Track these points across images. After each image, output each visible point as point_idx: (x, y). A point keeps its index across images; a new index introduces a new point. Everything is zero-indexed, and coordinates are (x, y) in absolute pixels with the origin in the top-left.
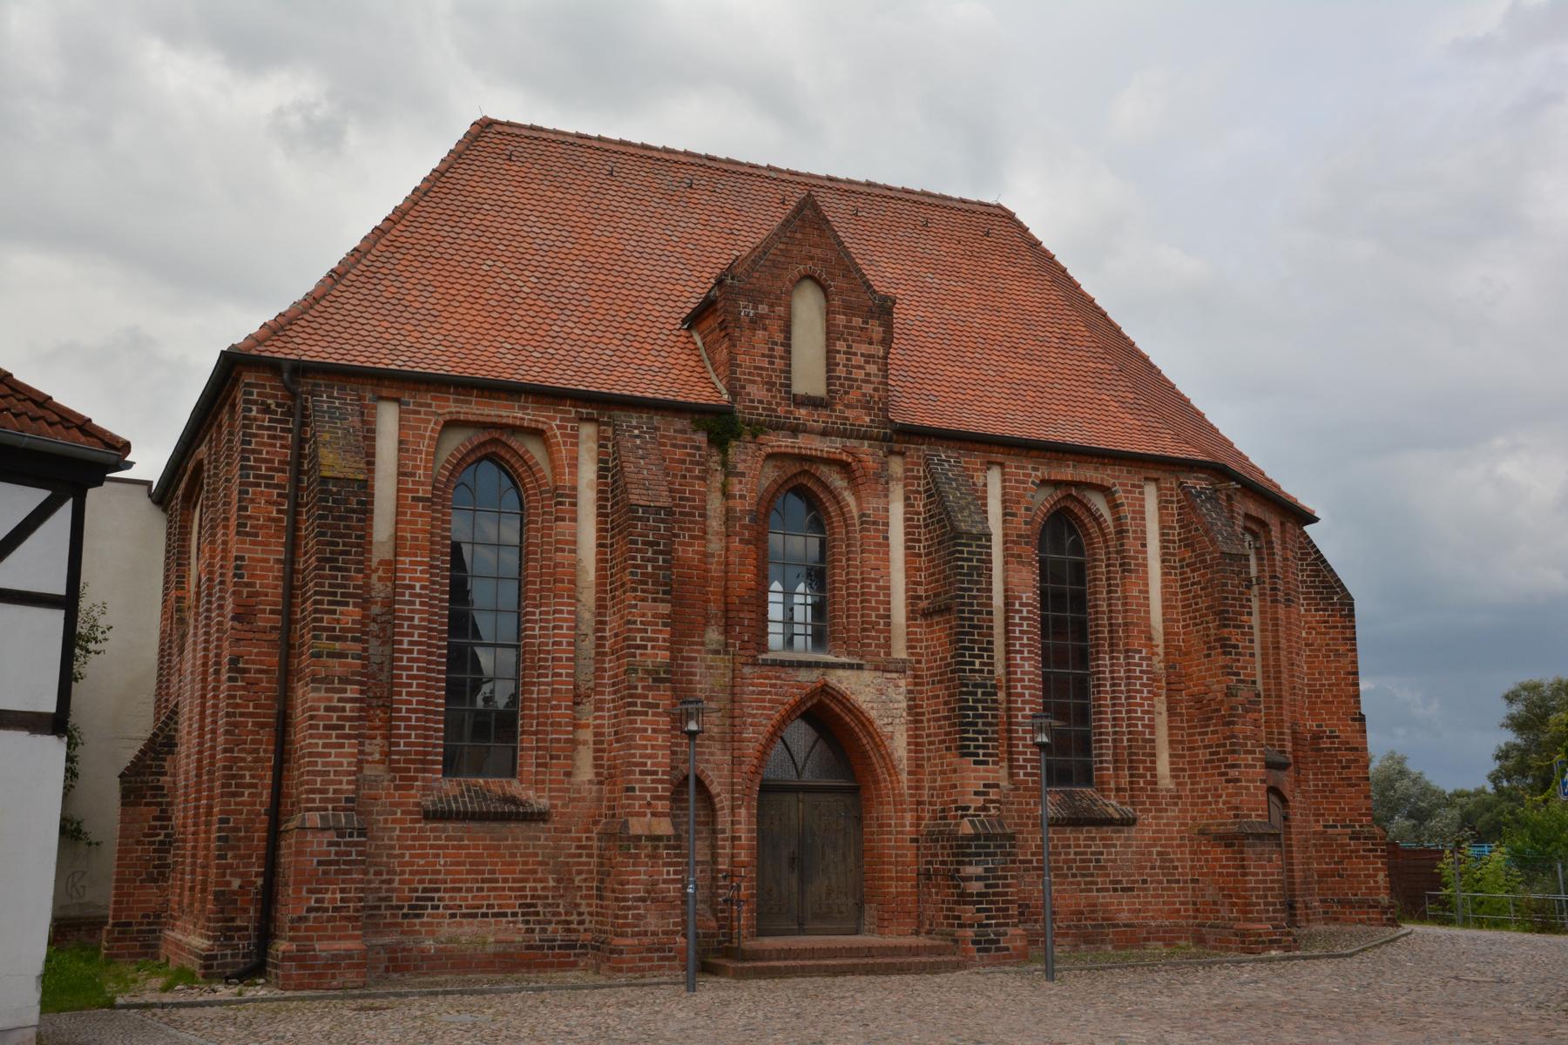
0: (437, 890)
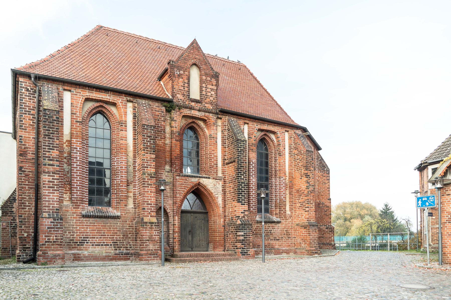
0: (88, 238)
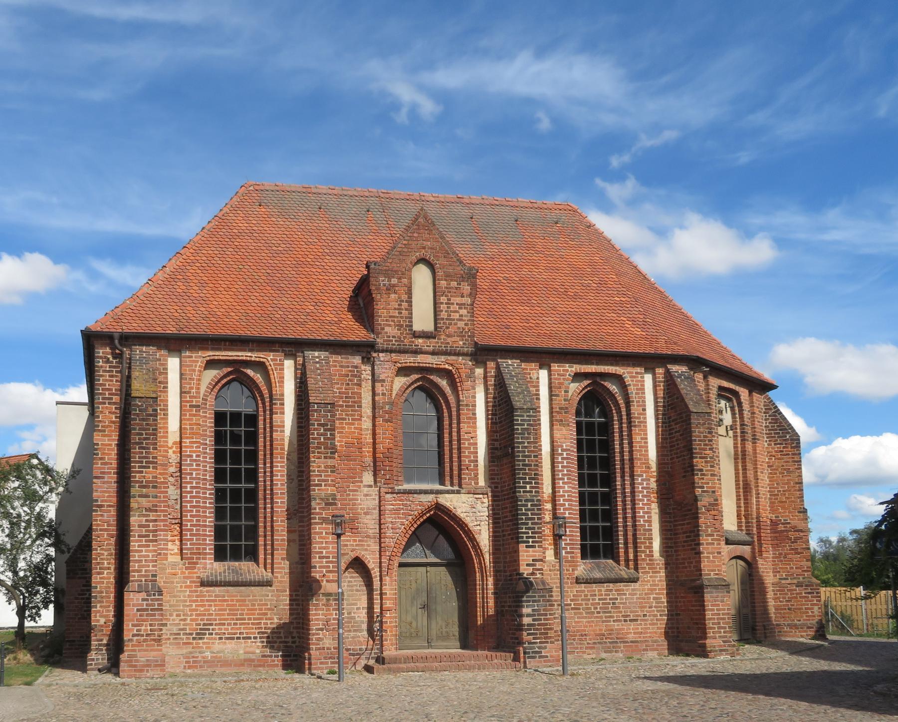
0: (211, 625)
